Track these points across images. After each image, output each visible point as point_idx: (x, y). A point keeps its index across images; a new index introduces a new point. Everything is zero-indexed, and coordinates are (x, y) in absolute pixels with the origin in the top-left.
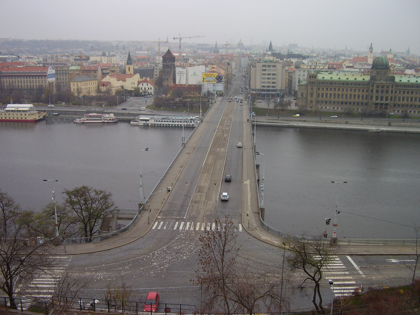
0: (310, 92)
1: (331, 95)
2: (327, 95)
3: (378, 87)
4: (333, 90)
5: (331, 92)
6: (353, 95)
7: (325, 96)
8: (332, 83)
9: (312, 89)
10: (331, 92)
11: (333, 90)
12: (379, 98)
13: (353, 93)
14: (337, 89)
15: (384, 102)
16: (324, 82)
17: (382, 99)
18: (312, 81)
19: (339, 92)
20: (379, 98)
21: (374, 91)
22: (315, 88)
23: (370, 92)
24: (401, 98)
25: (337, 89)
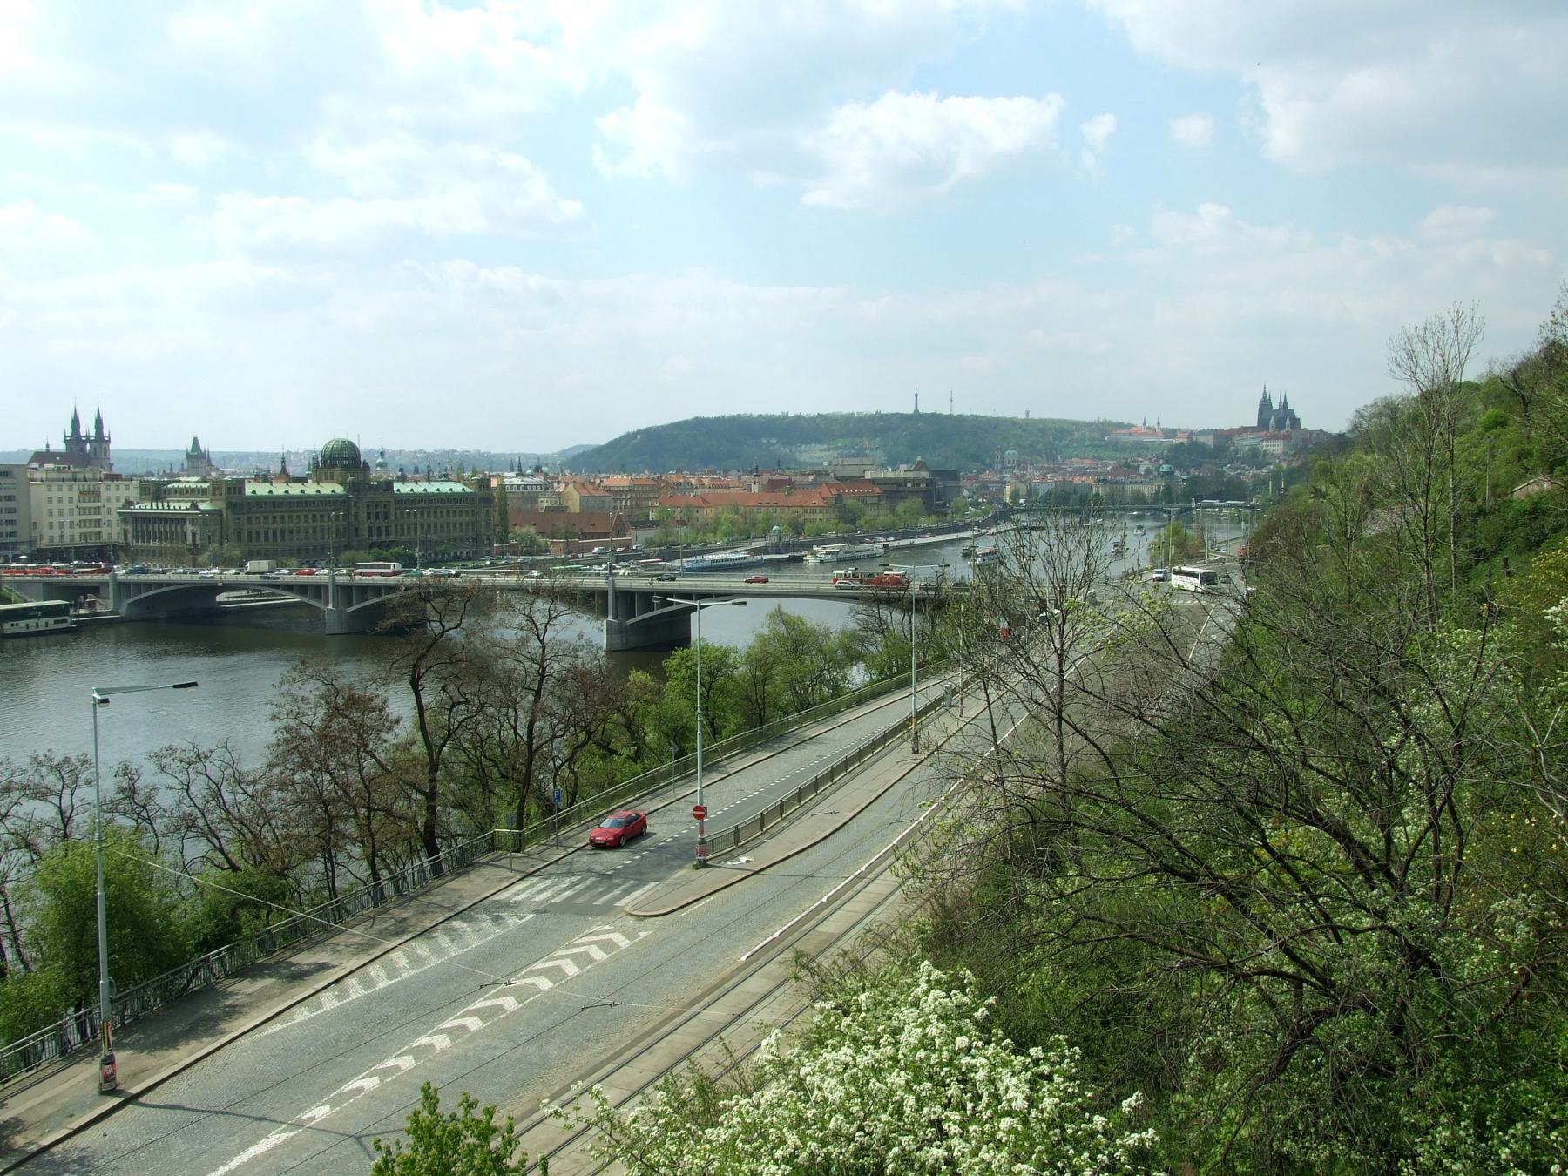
0: (235, 529)
1: (275, 532)
2: (267, 533)
3: (368, 507)
4: (278, 520)
5: (275, 526)
6: (318, 530)
7: (262, 536)
8: (272, 502)
9: (239, 519)
10: (275, 526)
11: (278, 520)
12: (375, 531)
13: (318, 524)
14: (287, 518)
15: (383, 538)
16: (259, 502)
17: (379, 535)
18: (234, 500)
19: (292, 525)
20: (375, 531)
21: (363, 516)
22: (244, 518)
23: (352, 519)
24: (406, 528)
25: (287, 518)
